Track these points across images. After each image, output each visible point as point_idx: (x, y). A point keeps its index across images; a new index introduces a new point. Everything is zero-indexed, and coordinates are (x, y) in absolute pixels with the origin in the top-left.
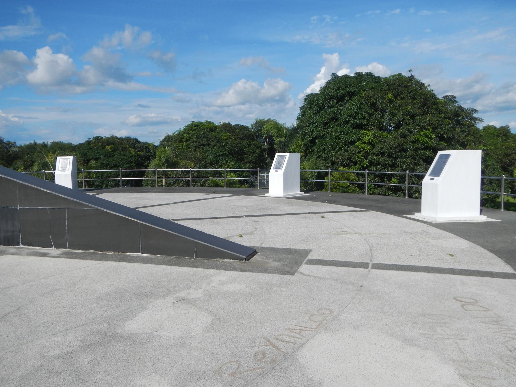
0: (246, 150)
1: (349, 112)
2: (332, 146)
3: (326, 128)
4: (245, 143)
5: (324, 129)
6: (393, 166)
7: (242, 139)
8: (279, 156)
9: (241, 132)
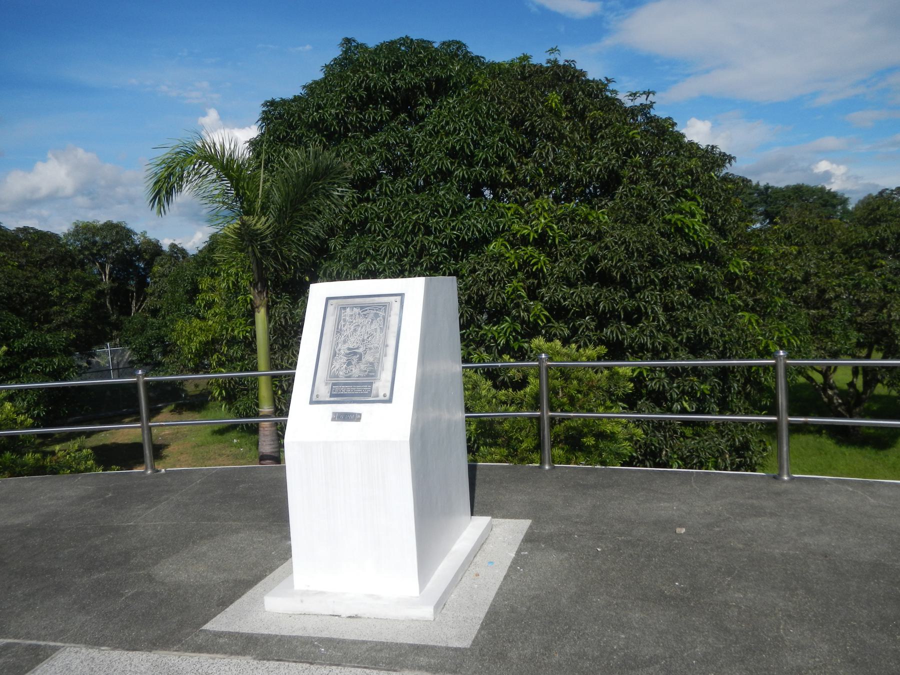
0: (56, 293)
1: (451, 141)
2: (399, 260)
3: (367, 200)
4: (51, 274)
5: (360, 200)
6: (634, 317)
7: (41, 265)
8: (343, 302)
9: (35, 249)
